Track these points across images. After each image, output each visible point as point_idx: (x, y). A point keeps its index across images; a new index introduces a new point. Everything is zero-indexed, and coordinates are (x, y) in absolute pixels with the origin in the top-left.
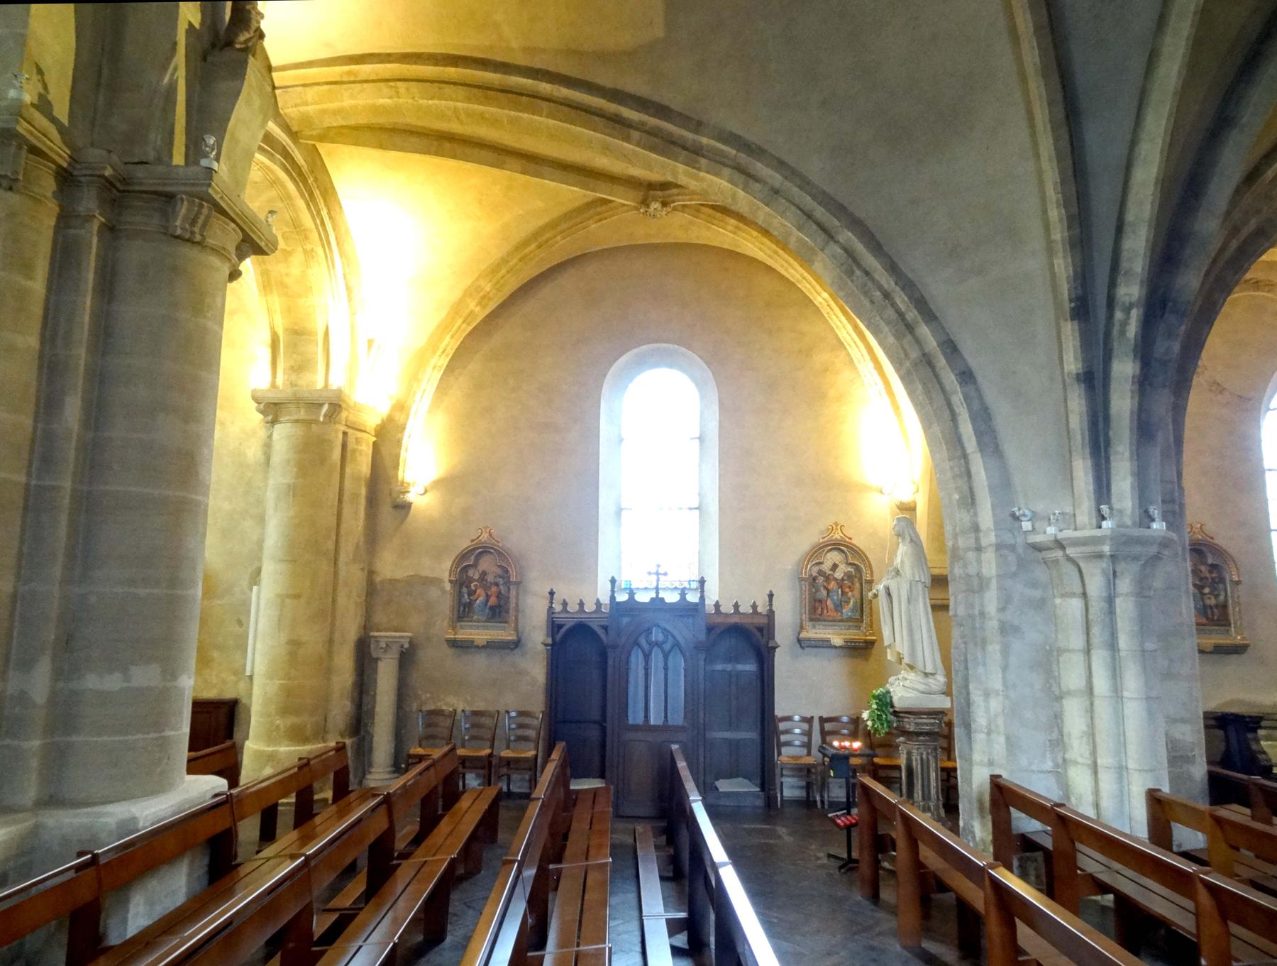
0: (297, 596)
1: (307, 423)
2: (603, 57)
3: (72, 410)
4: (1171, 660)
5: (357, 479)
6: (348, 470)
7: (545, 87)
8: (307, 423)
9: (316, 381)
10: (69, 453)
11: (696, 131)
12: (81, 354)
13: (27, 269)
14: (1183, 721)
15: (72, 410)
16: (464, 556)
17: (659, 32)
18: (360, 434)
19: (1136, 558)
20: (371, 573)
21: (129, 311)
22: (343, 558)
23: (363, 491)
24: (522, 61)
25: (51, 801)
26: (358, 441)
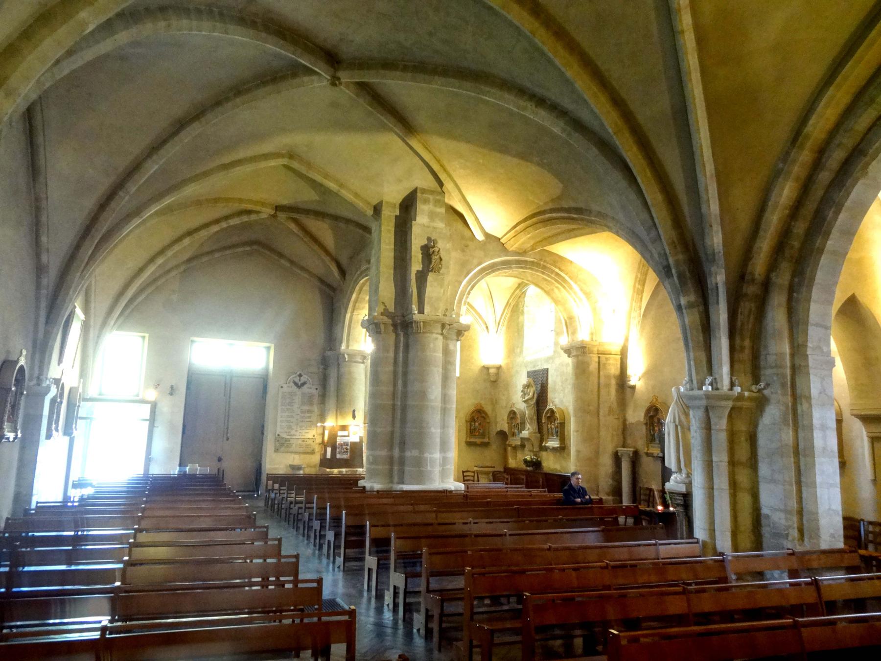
0: (577, 431)
1: (576, 356)
2: (559, 198)
3: (400, 382)
4: (773, 470)
5: (608, 377)
6: (601, 373)
7: (554, 215)
8: (576, 356)
9: (583, 336)
10: (399, 395)
11: (589, 216)
12: (400, 369)
13: (388, 351)
14: (781, 511)
15: (400, 382)
16: (648, 410)
17: (561, 185)
18: (607, 356)
19: (698, 408)
20: (625, 420)
21: (411, 355)
22: (601, 414)
23: (613, 382)
24: (547, 207)
25: (403, 483)
26: (607, 359)
